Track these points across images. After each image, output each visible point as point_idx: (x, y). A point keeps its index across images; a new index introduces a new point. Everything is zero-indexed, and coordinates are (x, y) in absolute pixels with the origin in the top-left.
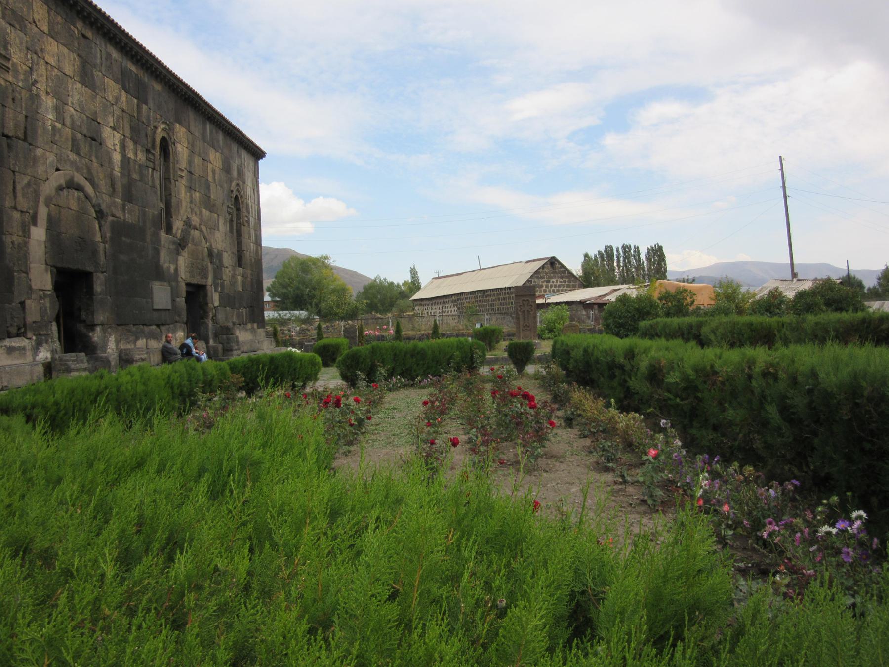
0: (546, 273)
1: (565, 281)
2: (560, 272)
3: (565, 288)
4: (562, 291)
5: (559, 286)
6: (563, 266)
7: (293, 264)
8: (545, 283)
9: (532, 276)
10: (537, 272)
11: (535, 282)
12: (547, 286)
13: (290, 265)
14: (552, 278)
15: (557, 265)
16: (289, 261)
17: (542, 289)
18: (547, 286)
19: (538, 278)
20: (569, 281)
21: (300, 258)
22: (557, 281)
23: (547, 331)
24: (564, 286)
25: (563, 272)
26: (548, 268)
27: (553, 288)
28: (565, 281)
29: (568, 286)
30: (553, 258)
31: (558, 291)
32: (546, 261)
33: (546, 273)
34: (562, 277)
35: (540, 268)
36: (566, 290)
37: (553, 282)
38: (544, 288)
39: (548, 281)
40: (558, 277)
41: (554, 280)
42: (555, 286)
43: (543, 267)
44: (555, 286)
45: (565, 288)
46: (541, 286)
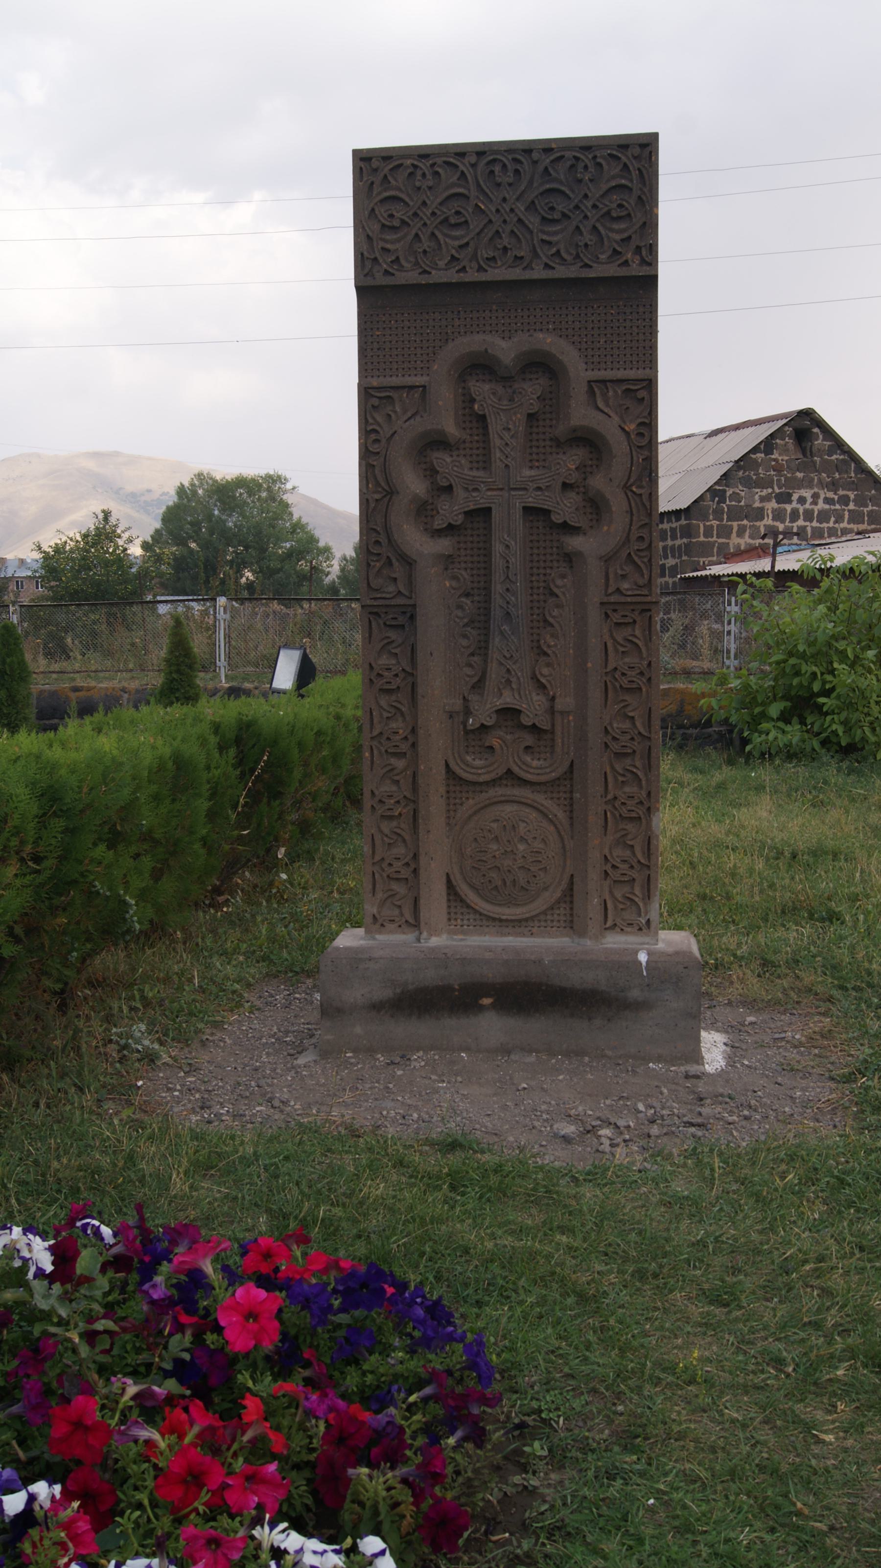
0: (778, 469)
1: (845, 500)
2: (827, 467)
3: (844, 525)
4: (832, 532)
5: (823, 516)
6: (839, 445)
7: (200, 492)
8: (773, 504)
9: (725, 476)
10: (744, 462)
11: (736, 497)
12: (778, 516)
13: (194, 493)
14: (800, 485)
15: (820, 442)
16: (192, 485)
17: (762, 525)
18: (778, 516)
19: (748, 483)
20: (861, 501)
21: (218, 477)
22: (815, 496)
23: (774, 710)
24: (839, 519)
25: (840, 467)
26: (785, 451)
27: (801, 522)
28: (845, 500)
29: (856, 517)
30: (807, 414)
31: (818, 533)
32: (784, 421)
33: (778, 469)
34: (833, 486)
35: (755, 450)
36: (845, 532)
37: (802, 500)
38: (768, 521)
39: (785, 498)
40: (821, 484)
41: (807, 494)
42: (808, 516)
43: (767, 445)
44: (808, 516)
45: (844, 525)
46: (760, 514)
